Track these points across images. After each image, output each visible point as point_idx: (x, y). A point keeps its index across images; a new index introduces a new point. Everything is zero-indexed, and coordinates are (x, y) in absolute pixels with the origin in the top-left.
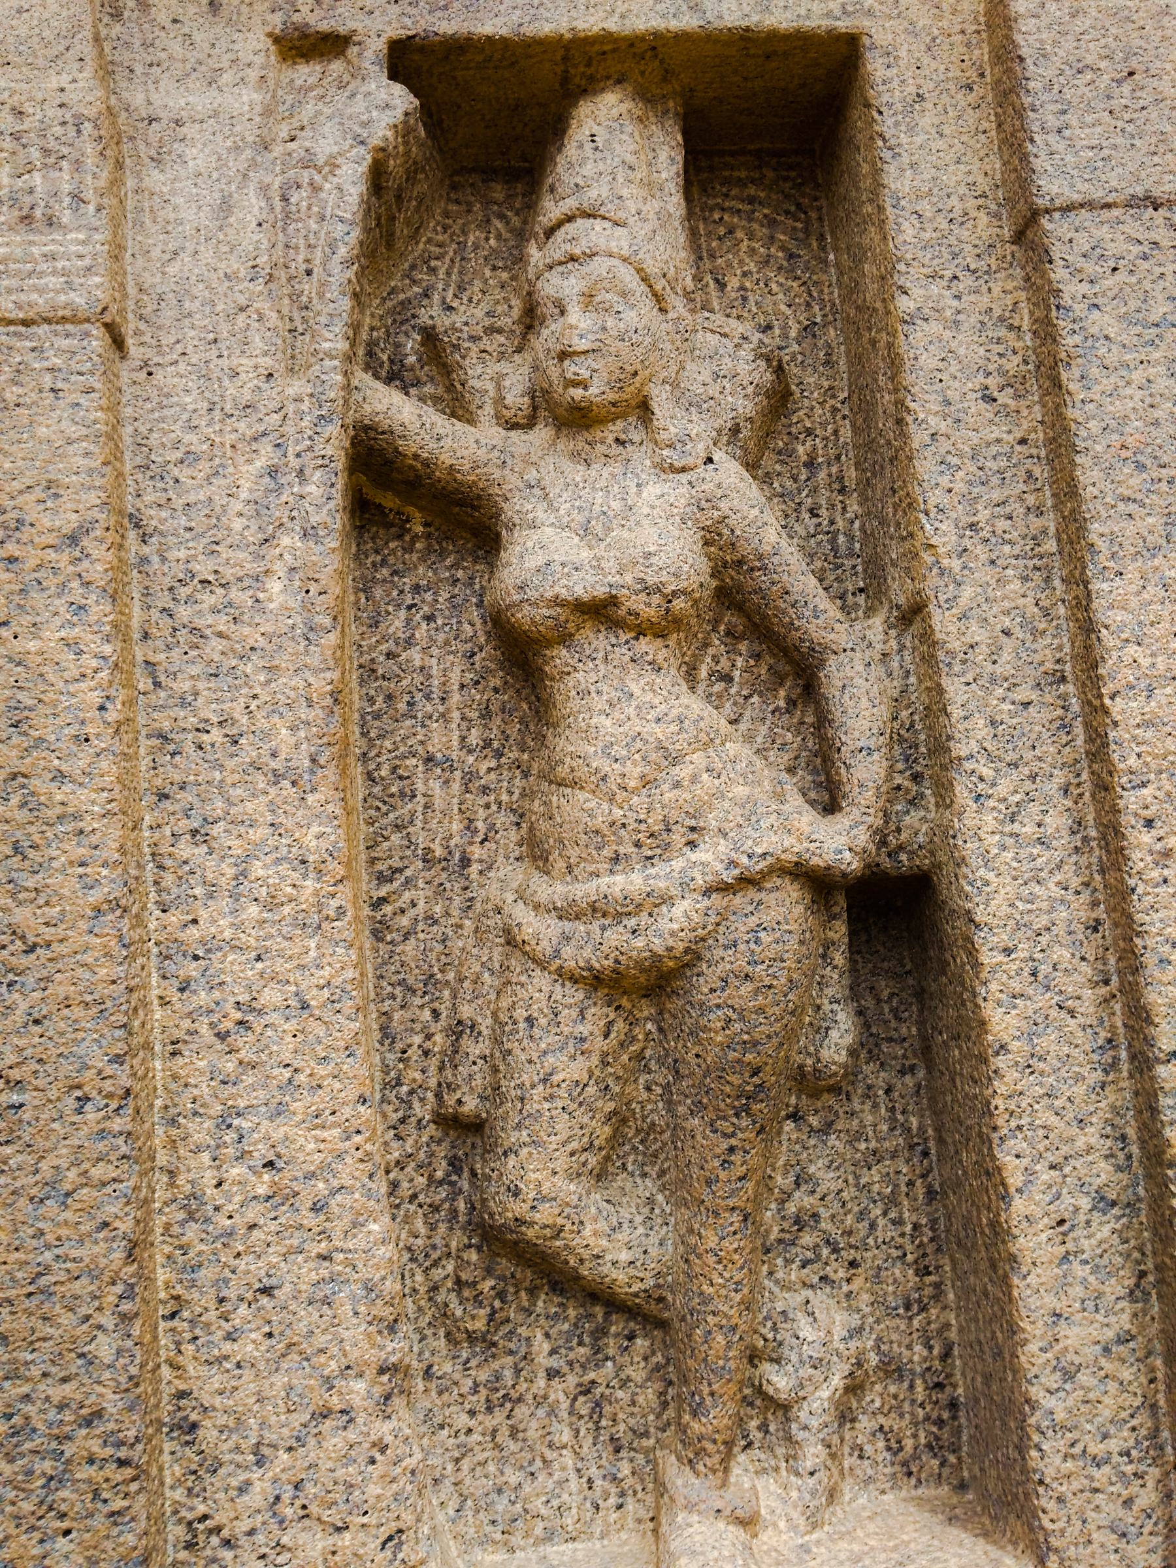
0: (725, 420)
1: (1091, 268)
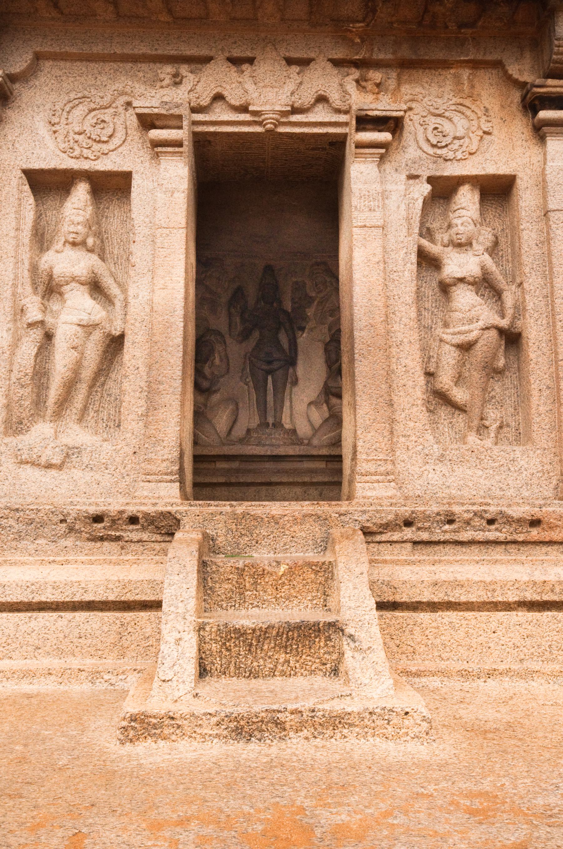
0: (486, 247)
1: (557, 222)
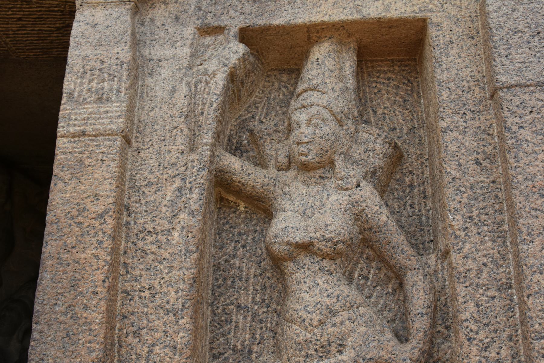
0: (371, 168)
1: (520, 111)
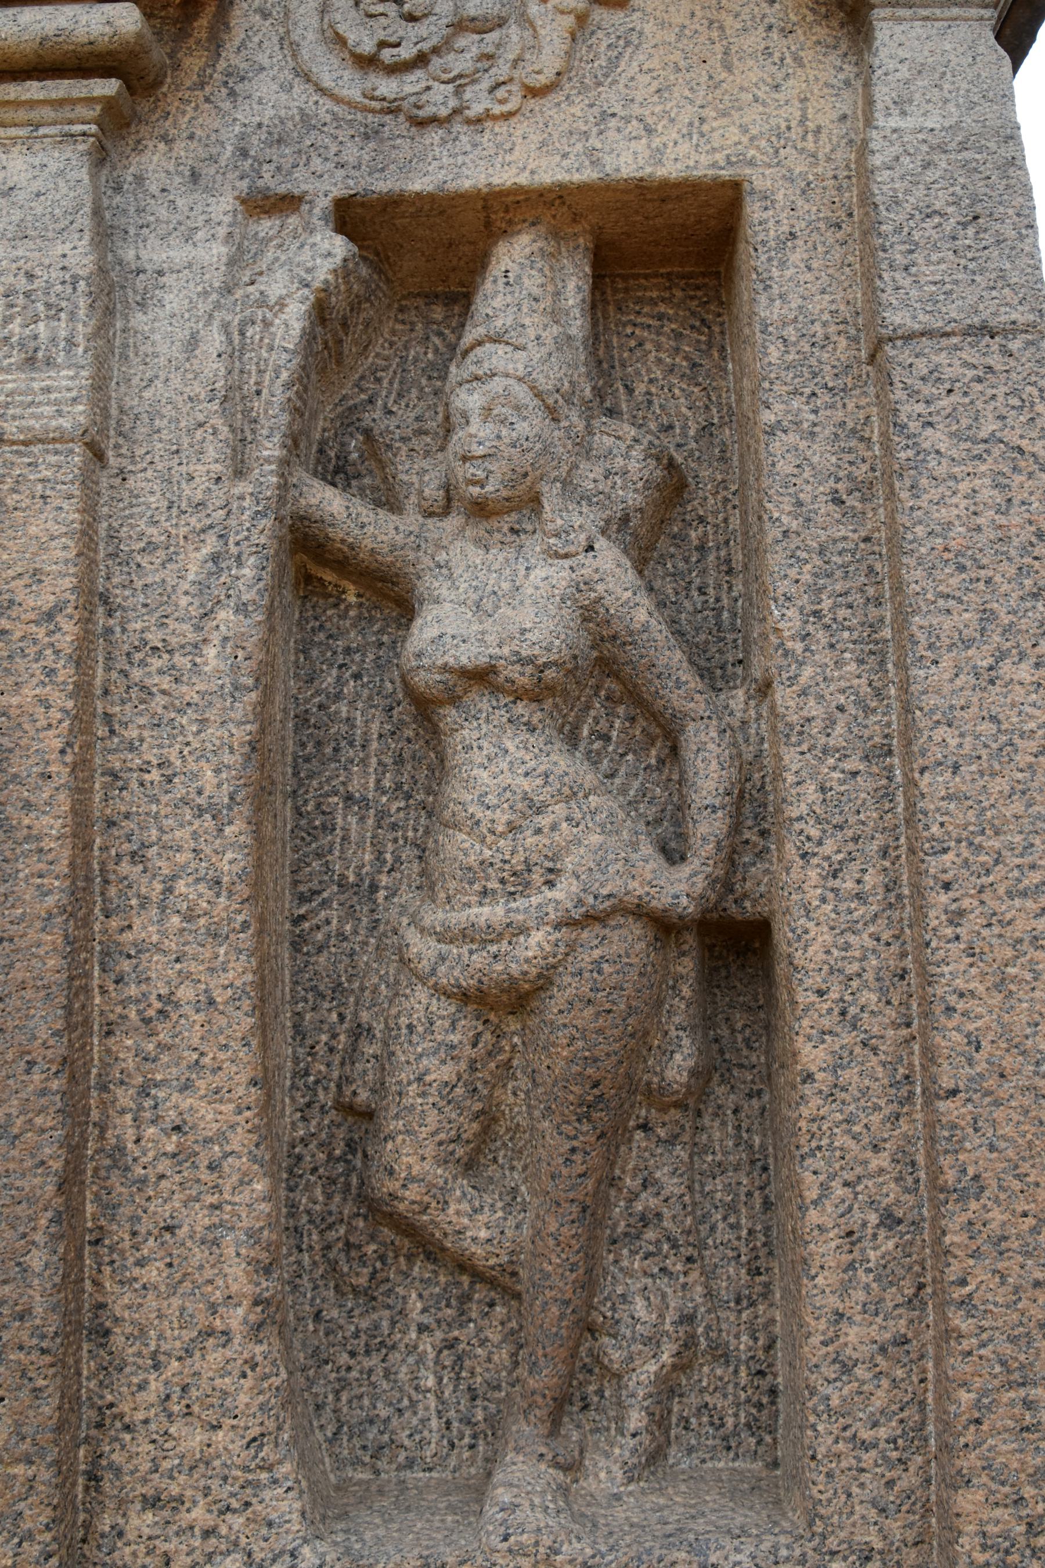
1: (927, 390)
